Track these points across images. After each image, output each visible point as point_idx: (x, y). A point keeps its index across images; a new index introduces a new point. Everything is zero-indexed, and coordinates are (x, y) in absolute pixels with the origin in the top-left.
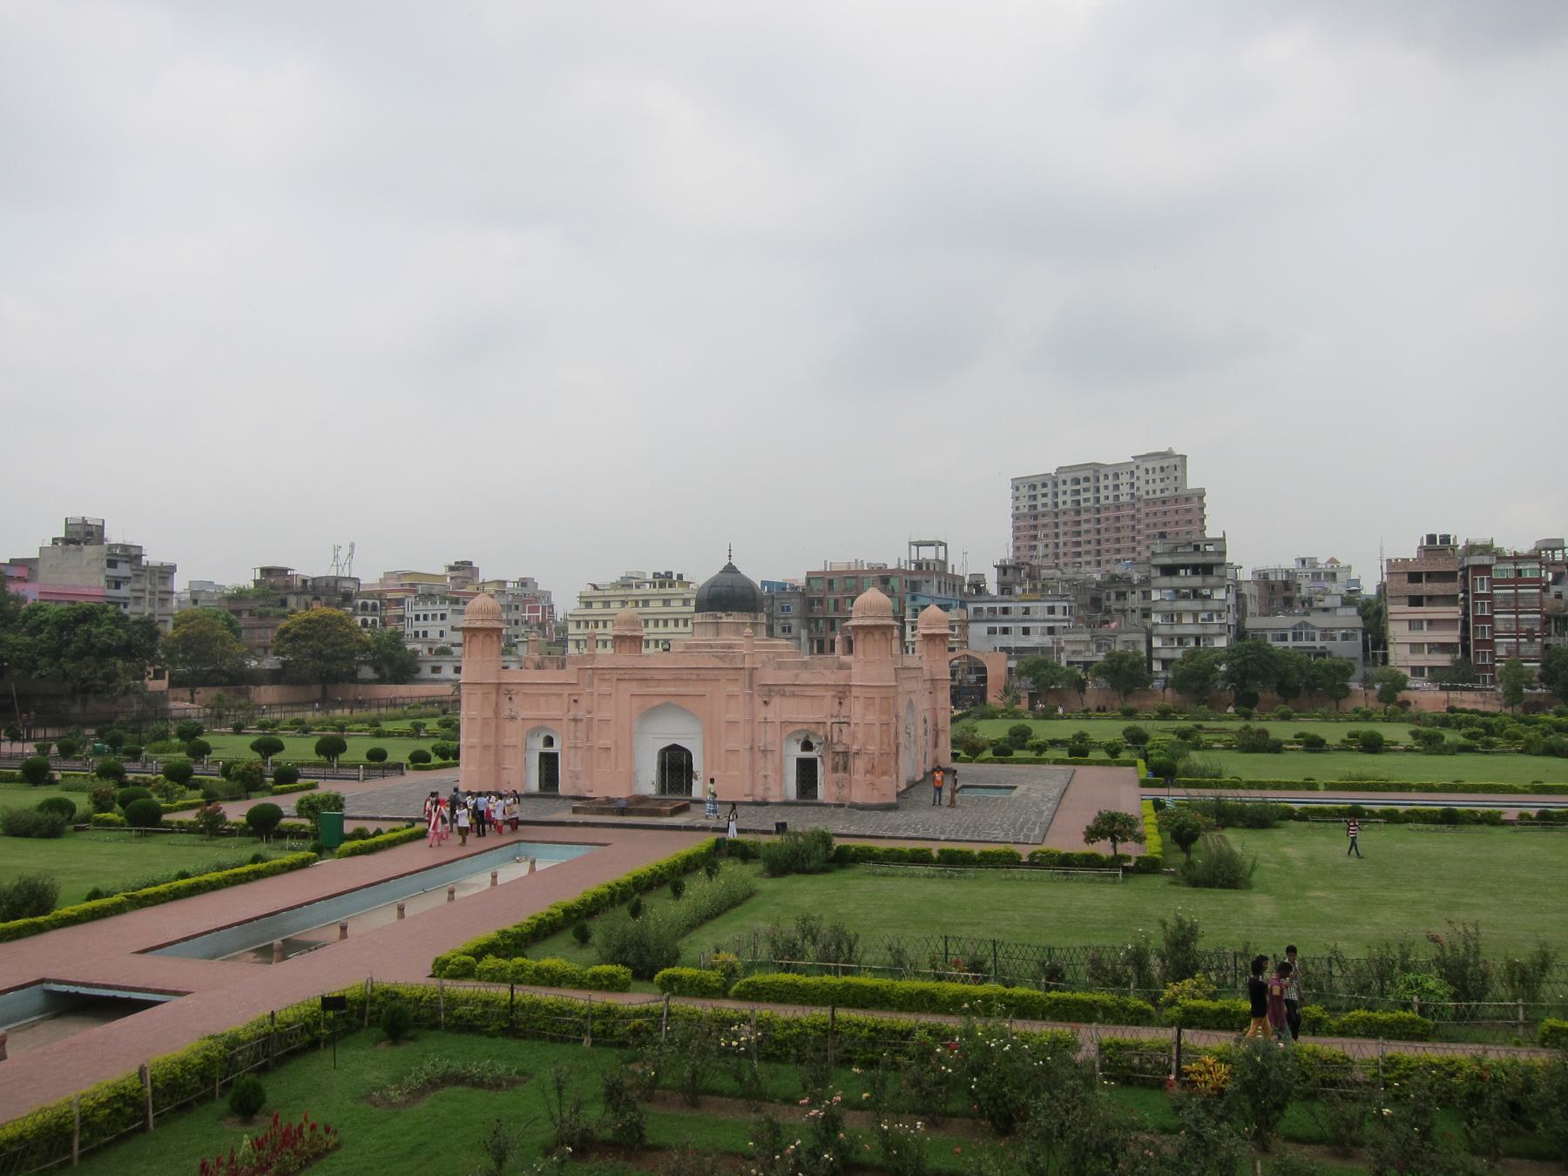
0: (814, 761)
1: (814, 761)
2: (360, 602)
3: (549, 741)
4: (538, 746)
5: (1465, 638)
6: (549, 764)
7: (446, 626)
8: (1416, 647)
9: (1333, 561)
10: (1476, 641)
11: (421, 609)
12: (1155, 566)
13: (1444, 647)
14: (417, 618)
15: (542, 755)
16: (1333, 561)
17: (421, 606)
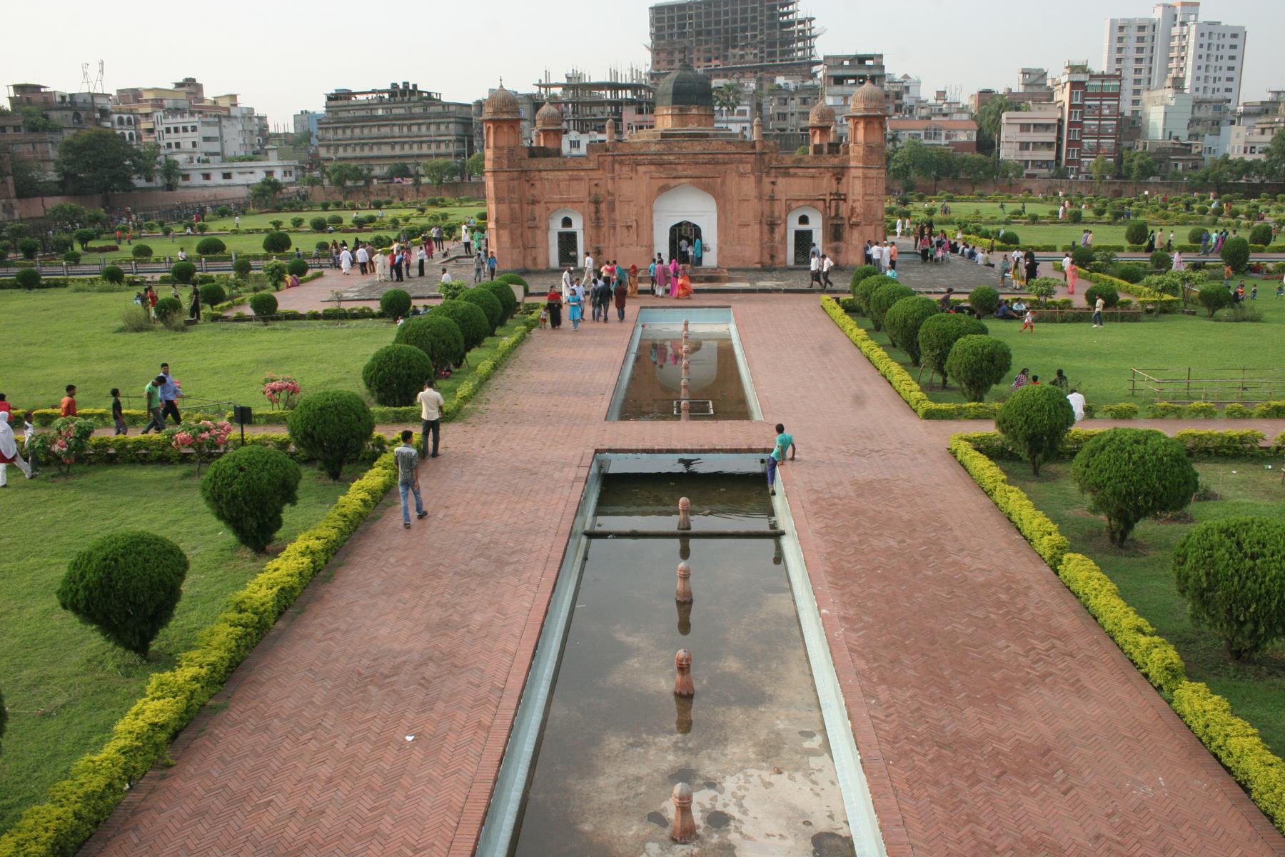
0: (810, 233)
1: (810, 233)
2: (116, 117)
3: (567, 222)
4: (556, 227)
5: (1059, 138)
6: (567, 241)
7: (196, 137)
8: (1024, 146)
9: (906, 77)
10: (1069, 141)
11: (172, 121)
12: (829, 77)
13: (1049, 145)
14: (168, 130)
15: (560, 235)
16: (906, 77)
17: (170, 120)
